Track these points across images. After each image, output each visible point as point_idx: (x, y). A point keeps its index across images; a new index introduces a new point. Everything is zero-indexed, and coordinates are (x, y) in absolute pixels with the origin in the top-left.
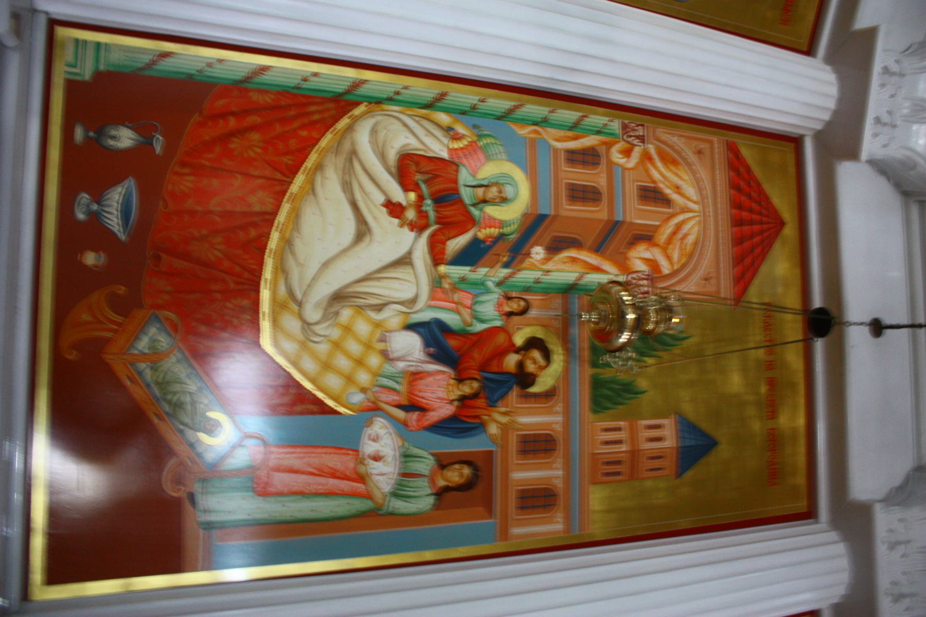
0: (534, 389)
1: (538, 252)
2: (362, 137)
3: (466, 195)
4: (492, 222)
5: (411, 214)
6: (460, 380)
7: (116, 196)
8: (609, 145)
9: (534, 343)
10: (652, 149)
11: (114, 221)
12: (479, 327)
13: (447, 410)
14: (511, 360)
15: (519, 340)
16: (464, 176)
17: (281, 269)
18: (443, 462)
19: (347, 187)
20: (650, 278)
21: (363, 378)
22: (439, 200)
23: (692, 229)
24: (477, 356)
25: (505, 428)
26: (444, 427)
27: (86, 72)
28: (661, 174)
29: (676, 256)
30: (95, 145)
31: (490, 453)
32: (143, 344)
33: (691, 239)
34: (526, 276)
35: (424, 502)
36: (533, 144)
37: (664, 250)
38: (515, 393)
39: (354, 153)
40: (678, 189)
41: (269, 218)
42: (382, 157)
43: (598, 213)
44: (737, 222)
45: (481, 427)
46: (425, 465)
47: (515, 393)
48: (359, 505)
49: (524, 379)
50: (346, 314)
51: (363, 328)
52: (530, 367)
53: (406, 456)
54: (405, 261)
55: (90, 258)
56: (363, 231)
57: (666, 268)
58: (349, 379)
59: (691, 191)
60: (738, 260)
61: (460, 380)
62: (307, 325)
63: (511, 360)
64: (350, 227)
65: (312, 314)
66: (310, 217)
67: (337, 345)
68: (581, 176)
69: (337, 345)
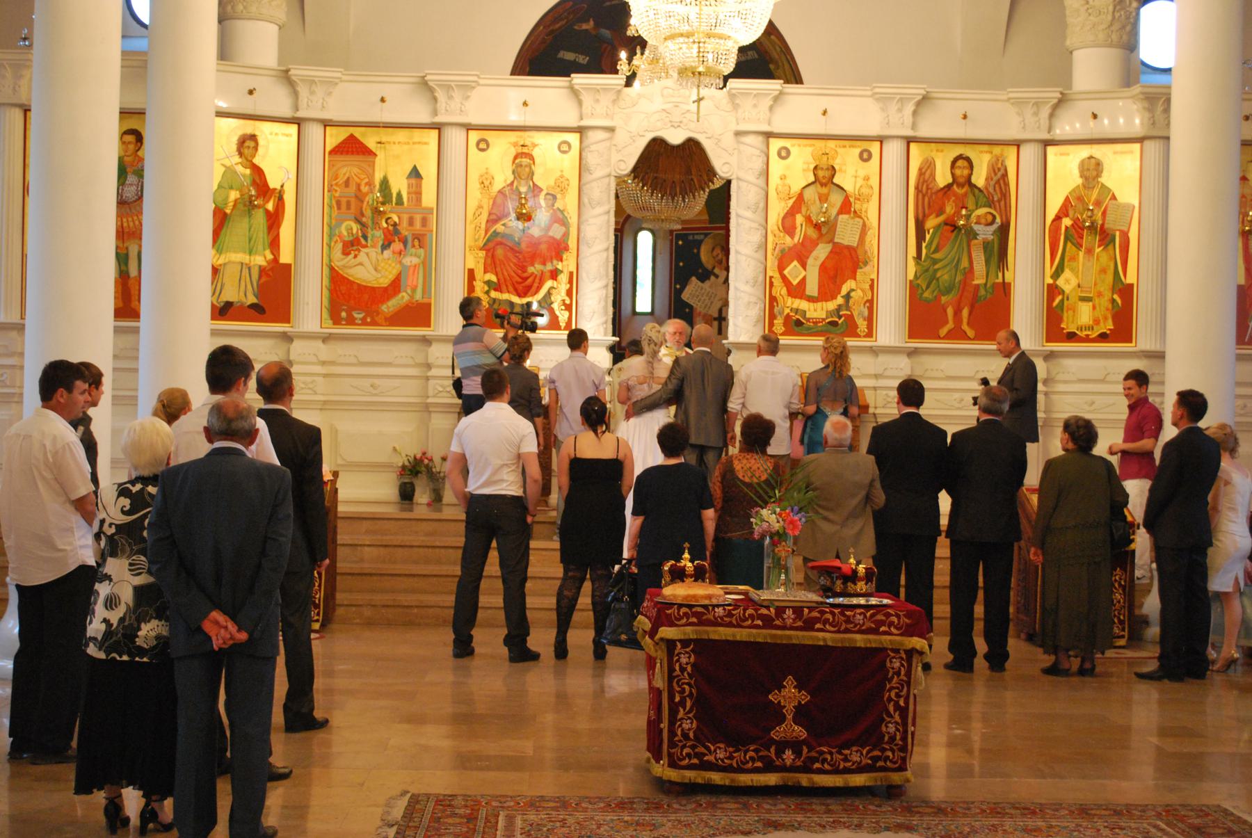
0: (398, 222)
1: (364, 220)
2: (339, 264)
3: (351, 238)
4: (357, 232)
5: (356, 253)
6: (394, 241)
7: (356, 315)
8: (335, 197)
9: (386, 222)
10: (334, 182)
11: (361, 316)
12: (383, 236)
13: (402, 244)
14: (391, 228)
15: (385, 225)
16: (347, 239)
17: (370, 282)
18: (413, 246)
19: (351, 267)
20: (370, 185)
21: (393, 265)
22: (353, 245)
23: (356, 170)
24: (389, 237)
25: (407, 230)
26: (405, 246)
27: (331, 322)
28: (341, 180)
29: (363, 176)
30: (346, 320)
31: (413, 234)
32: (386, 310)
33: (358, 170)
34: (370, 223)
35: (421, 251)
36: (336, 220)
37: (362, 180)
38: (398, 227)
39: (344, 266)
40: (345, 174)
41: (359, 285)
42: (343, 259)
43: (353, 201)
44: (352, 153)
45: (406, 236)
46: (413, 250)
47: (398, 227)
48: (421, 265)
49: (395, 225)
50: (380, 268)
51: (382, 265)
52: (392, 223)
53: (411, 255)
54: (367, 254)
55: (369, 320)
56: (361, 264)
57: (367, 180)
58: (394, 268)
59: (344, 170)
60: (364, 153)
61: (394, 241)
62: (382, 277)
63: (391, 228)
64: (360, 267)
65: (379, 275)
66: (359, 276)
67: (386, 270)
68: (344, 206)
69: (386, 270)
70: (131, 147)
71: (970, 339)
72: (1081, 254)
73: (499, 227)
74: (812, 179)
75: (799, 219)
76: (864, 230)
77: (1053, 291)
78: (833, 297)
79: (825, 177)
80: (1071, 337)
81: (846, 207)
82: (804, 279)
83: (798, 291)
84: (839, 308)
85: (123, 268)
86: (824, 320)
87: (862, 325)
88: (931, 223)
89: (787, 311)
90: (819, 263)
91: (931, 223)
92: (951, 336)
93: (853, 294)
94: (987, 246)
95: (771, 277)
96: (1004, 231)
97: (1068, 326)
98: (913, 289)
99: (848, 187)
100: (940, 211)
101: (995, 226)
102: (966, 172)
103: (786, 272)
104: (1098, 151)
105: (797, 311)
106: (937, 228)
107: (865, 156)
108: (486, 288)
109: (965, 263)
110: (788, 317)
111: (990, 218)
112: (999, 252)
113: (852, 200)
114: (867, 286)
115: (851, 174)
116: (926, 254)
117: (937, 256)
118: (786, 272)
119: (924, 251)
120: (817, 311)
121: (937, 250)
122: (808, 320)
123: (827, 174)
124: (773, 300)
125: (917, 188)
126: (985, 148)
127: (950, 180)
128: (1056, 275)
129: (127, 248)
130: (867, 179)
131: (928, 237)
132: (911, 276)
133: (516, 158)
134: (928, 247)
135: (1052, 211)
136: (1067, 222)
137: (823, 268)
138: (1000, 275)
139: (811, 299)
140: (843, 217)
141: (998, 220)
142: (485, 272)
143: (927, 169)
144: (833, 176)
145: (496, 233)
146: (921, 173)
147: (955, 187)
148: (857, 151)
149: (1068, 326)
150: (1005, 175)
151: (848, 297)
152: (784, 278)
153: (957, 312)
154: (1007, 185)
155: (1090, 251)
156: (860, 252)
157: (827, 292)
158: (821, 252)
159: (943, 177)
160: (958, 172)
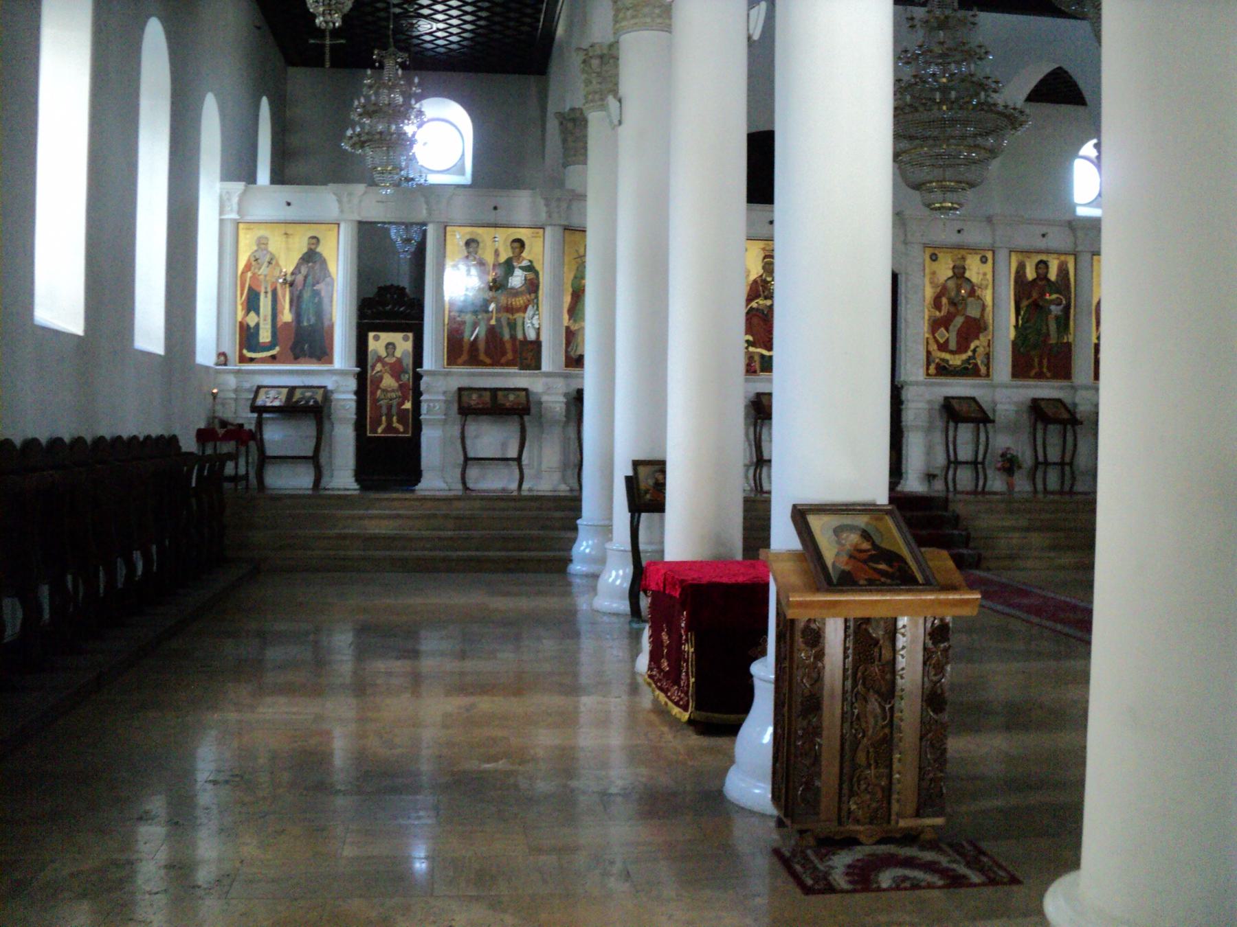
70: (517, 250)
71: (1047, 378)
73: (754, 304)
74: (950, 273)
75: (944, 300)
76: (984, 307)
78: (966, 351)
79: (959, 273)
81: (972, 293)
82: (948, 339)
83: (943, 347)
84: (970, 358)
85: (513, 332)
86: (959, 366)
87: (983, 370)
88: (1024, 303)
89: (937, 360)
90: (956, 328)
91: (1024, 303)
93: (978, 349)
94: (1057, 318)
95: (927, 338)
96: (1067, 308)
98: (1014, 344)
99: (974, 280)
101: (1062, 306)
102: (1045, 271)
103: (936, 335)
105: (943, 360)
106: (1027, 306)
107: (984, 260)
108: (746, 345)
109: (1044, 331)
110: (938, 364)
111: (1059, 300)
113: (976, 288)
114: (986, 344)
115: (975, 271)
116: (1022, 324)
117: (1028, 325)
118: (936, 335)
119: (1020, 322)
120: (956, 361)
121: (1027, 322)
122: (950, 366)
123: (962, 271)
124: (929, 353)
126: (1055, 256)
127: (1035, 275)
129: (515, 319)
130: (985, 274)
131: (1022, 313)
133: (764, 258)
134: (1022, 319)
137: (959, 333)
138: (1065, 337)
139: (952, 352)
140: (971, 299)
141: (1064, 302)
142: (746, 334)
144: (964, 273)
145: (752, 309)
146: (1017, 272)
148: (978, 258)
150: (1067, 273)
151: (974, 351)
152: (935, 338)
153: (1040, 363)
154: (1068, 280)
156: (982, 323)
157: (962, 347)
158: (959, 321)
159: (1030, 274)
160: (1040, 271)
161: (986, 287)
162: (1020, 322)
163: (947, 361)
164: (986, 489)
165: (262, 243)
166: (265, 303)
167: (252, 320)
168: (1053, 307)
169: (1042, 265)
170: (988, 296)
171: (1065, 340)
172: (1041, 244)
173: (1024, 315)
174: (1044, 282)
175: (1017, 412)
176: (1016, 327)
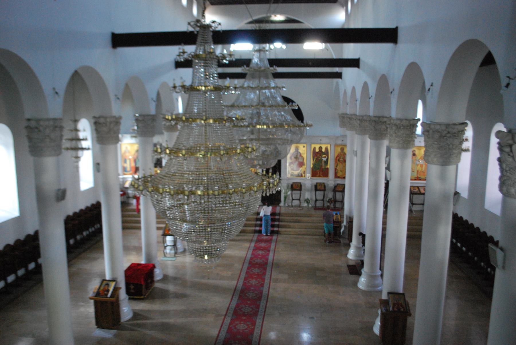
71: (321, 177)
72: (340, 164)
76: (303, 159)
77: (336, 169)
80: (339, 177)
87: (303, 175)
88: (316, 157)
92: (318, 177)
96: (327, 159)
97: (338, 175)
98: (312, 169)
100: (317, 156)
104: (343, 146)
109: (321, 164)
112: (326, 162)
114: (304, 168)
116: (315, 163)
125: (313, 152)
128: (336, 166)
131: (315, 160)
132: (312, 166)
134: (315, 162)
135: (336, 156)
136: (338, 158)
139: (295, 171)
143: (315, 148)
147: (320, 152)
149: (338, 175)
153: (320, 172)
155: (342, 163)
159: (317, 150)
161: (304, 154)
162: (314, 163)
163: (293, 173)
164: (301, 205)
165: (126, 148)
166: (128, 162)
167: (125, 165)
168: (323, 159)
169: (320, 148)
170: (305, 156)
171: (327, 167)
172: (319, 142)
173: (315, 161)
174: (320, 152)
175: (312, 186)
176: (313, 164)
